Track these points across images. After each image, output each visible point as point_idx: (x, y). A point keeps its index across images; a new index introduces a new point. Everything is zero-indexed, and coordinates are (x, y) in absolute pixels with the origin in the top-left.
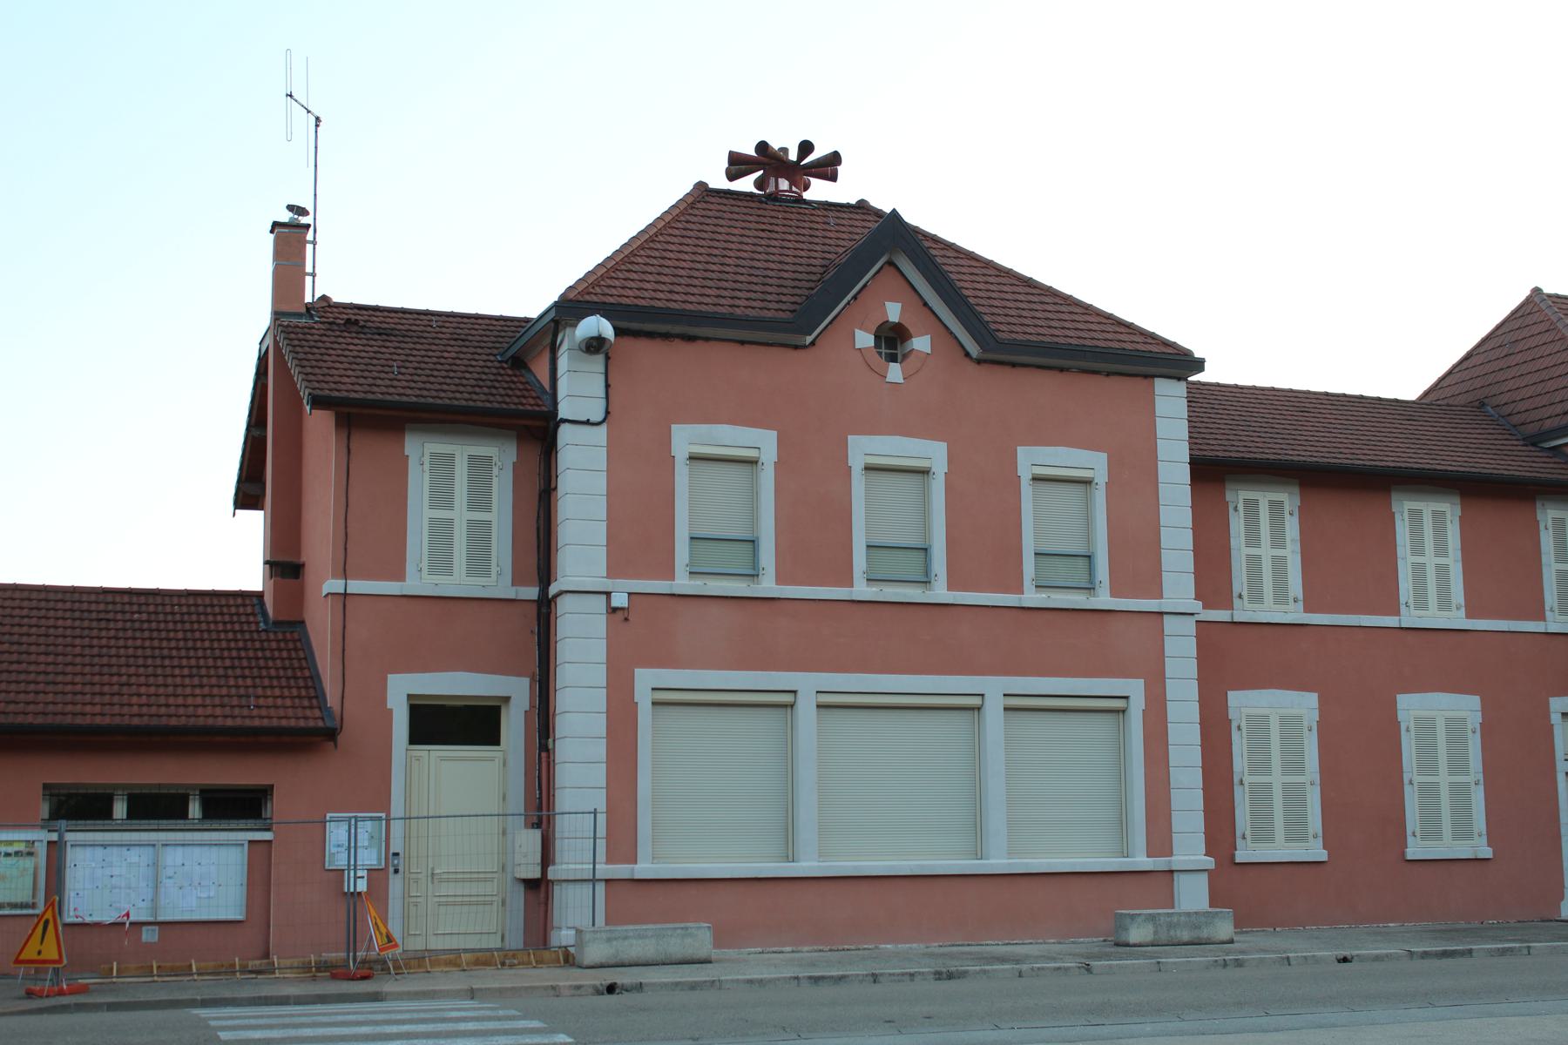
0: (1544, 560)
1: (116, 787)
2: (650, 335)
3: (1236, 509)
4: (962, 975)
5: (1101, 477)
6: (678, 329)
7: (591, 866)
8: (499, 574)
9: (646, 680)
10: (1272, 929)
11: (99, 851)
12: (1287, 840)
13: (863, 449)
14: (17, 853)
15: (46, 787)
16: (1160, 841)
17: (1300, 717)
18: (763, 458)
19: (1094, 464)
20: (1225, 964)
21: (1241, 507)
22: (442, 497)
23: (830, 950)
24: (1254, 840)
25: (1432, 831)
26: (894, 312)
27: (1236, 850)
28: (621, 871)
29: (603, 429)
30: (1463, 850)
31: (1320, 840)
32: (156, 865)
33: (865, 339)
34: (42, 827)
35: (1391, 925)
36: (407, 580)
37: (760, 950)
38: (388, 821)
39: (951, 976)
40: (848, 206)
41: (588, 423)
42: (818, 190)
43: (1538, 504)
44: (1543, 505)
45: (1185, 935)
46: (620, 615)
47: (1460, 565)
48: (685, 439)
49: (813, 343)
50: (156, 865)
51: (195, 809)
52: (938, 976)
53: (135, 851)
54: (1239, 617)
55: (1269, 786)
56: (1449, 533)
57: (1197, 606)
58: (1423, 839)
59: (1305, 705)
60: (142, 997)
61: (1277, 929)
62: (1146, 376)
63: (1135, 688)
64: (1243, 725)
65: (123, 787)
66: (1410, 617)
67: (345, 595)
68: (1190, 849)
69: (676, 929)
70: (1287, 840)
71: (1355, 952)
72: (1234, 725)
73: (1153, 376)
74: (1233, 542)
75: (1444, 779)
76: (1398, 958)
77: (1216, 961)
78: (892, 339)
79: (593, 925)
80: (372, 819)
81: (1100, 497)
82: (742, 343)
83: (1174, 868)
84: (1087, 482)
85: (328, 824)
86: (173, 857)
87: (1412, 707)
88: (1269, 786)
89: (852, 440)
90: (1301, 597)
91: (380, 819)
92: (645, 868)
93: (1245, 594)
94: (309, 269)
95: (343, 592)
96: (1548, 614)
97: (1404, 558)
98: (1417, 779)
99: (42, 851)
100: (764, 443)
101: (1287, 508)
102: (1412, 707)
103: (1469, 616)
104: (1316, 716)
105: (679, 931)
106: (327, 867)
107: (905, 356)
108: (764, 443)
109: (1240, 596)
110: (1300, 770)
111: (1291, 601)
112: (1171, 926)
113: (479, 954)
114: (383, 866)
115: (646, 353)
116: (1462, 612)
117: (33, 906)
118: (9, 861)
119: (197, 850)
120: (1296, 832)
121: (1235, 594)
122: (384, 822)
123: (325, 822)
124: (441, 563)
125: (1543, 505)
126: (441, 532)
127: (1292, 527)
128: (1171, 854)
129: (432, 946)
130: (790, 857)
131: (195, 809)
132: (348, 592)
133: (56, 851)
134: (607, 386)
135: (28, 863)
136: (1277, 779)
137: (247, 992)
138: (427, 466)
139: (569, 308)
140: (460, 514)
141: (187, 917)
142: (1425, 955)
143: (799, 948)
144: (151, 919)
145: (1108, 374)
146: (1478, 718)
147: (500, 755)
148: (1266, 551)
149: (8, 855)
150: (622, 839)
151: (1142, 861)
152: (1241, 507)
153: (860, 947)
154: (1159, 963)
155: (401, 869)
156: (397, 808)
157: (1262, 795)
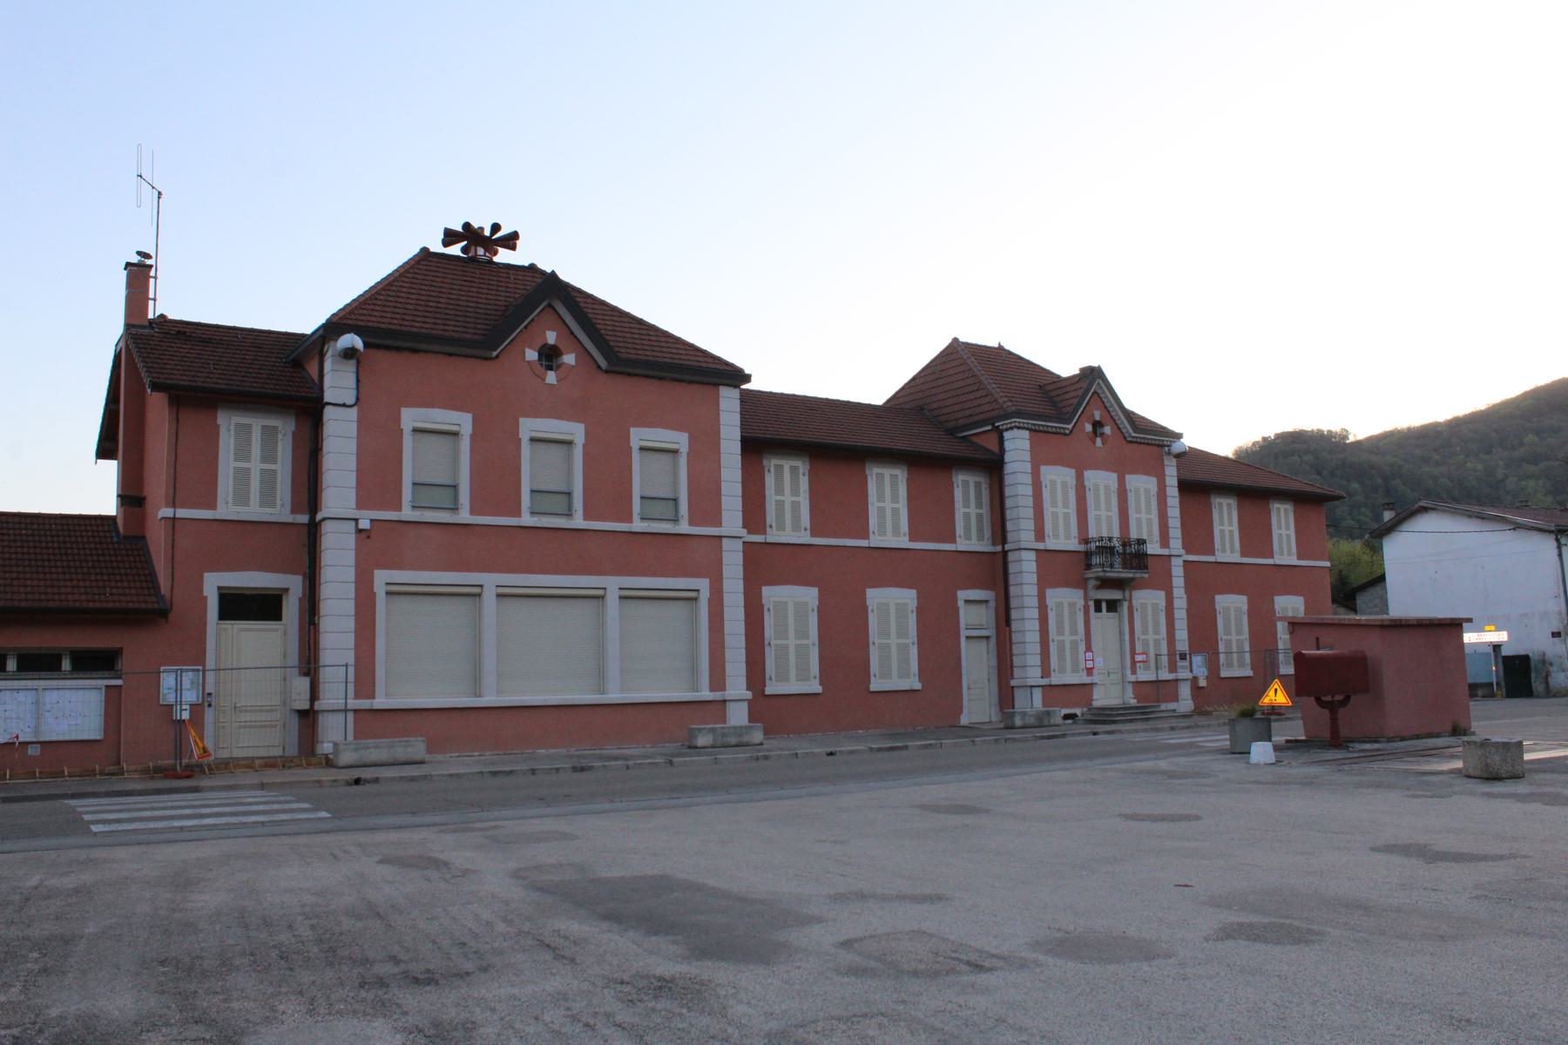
2: (388, 348)
3: (769, 471)
4: (590, 768)
6: (407, 344)
8: (282, 506)
9: (381, 578)
12: (797, 680)
13: (529, 427)
16: (718, 681)
17: (807, 603)
18: (462, 432)
19: (679, 440)
21: (772, 469)
22: (243, 453)
23: (505, 754)
25: (886, 674)
26: (551, 338)
28: (364, 704)
29: (355, 410)
30: (904, 685)
31: (818, 680)
33: (532, 355)
35: (860, 731)
36: (218, 508)
37: (457, 754)
38: (204, 671)
39: (582, 769)
41: (344, 405)
42: (503, 256)
43: (954, 472)
45: (733, 740)
46: (364, 535)
48: (411, 417)
49: (497, 356)
50: (37, 703)
51: (66, 665)
52: (575, 769)
53: (22, 694)
54: (770, 539)
58: (880, 678)
59: (810, 595)
60: (29, 793)
63: (703, 585)
66: (875, 541)
67: (174, 519)
68: (737, 686)
69: (400, 742)
70: (797, 680)
73: (717, 385)
74: (767, 492)
75: (894, 641)
78: (550, 356)
79: (346, 739)
80: (193, 670)
82: (450, 355)
83: (727, 698)
84: (675, 452)
85: (161, 674)
86: (51, 698)
87: (876, 597)
90: (808, 526)
91: (198, 670)
92: (380, 702)
93: (774, 524)
94: (151, 295)
95: (172, 516)
96: (958, 539)
97: (872, 504)
100: (463, 422)
101: (801, 471)
102: (876, 597)
105: (403, 743)
106: (161, 702)
107: (558, 367)
108: (463, 422)
109: (771, 526)
110: (805, 635)
111: (803, 529)
112: (724, 735)
114: (200, 702)
115: (384, 360)
116: (907, 538)
120: (803, 675)
124: (242, 497)
126: (242, 477)
127: (804, 484)
128: (724, 689)
129: (234, 755)
130: (477, 694)
131: (66, 665)
132: (177, 516)
138: (233, 433)
139: (333, 328)
140: (256, 465)
141: (61, 738)
142: (880, 750)
144: (34, 740)
145: (690, 382)
146: (915, 603)
148: (788, 498)
150: (364, 681)
151: (706, 694)
152: (772, 469)
154: (716, 758)
156: (210, 662)
157: (782, 651)
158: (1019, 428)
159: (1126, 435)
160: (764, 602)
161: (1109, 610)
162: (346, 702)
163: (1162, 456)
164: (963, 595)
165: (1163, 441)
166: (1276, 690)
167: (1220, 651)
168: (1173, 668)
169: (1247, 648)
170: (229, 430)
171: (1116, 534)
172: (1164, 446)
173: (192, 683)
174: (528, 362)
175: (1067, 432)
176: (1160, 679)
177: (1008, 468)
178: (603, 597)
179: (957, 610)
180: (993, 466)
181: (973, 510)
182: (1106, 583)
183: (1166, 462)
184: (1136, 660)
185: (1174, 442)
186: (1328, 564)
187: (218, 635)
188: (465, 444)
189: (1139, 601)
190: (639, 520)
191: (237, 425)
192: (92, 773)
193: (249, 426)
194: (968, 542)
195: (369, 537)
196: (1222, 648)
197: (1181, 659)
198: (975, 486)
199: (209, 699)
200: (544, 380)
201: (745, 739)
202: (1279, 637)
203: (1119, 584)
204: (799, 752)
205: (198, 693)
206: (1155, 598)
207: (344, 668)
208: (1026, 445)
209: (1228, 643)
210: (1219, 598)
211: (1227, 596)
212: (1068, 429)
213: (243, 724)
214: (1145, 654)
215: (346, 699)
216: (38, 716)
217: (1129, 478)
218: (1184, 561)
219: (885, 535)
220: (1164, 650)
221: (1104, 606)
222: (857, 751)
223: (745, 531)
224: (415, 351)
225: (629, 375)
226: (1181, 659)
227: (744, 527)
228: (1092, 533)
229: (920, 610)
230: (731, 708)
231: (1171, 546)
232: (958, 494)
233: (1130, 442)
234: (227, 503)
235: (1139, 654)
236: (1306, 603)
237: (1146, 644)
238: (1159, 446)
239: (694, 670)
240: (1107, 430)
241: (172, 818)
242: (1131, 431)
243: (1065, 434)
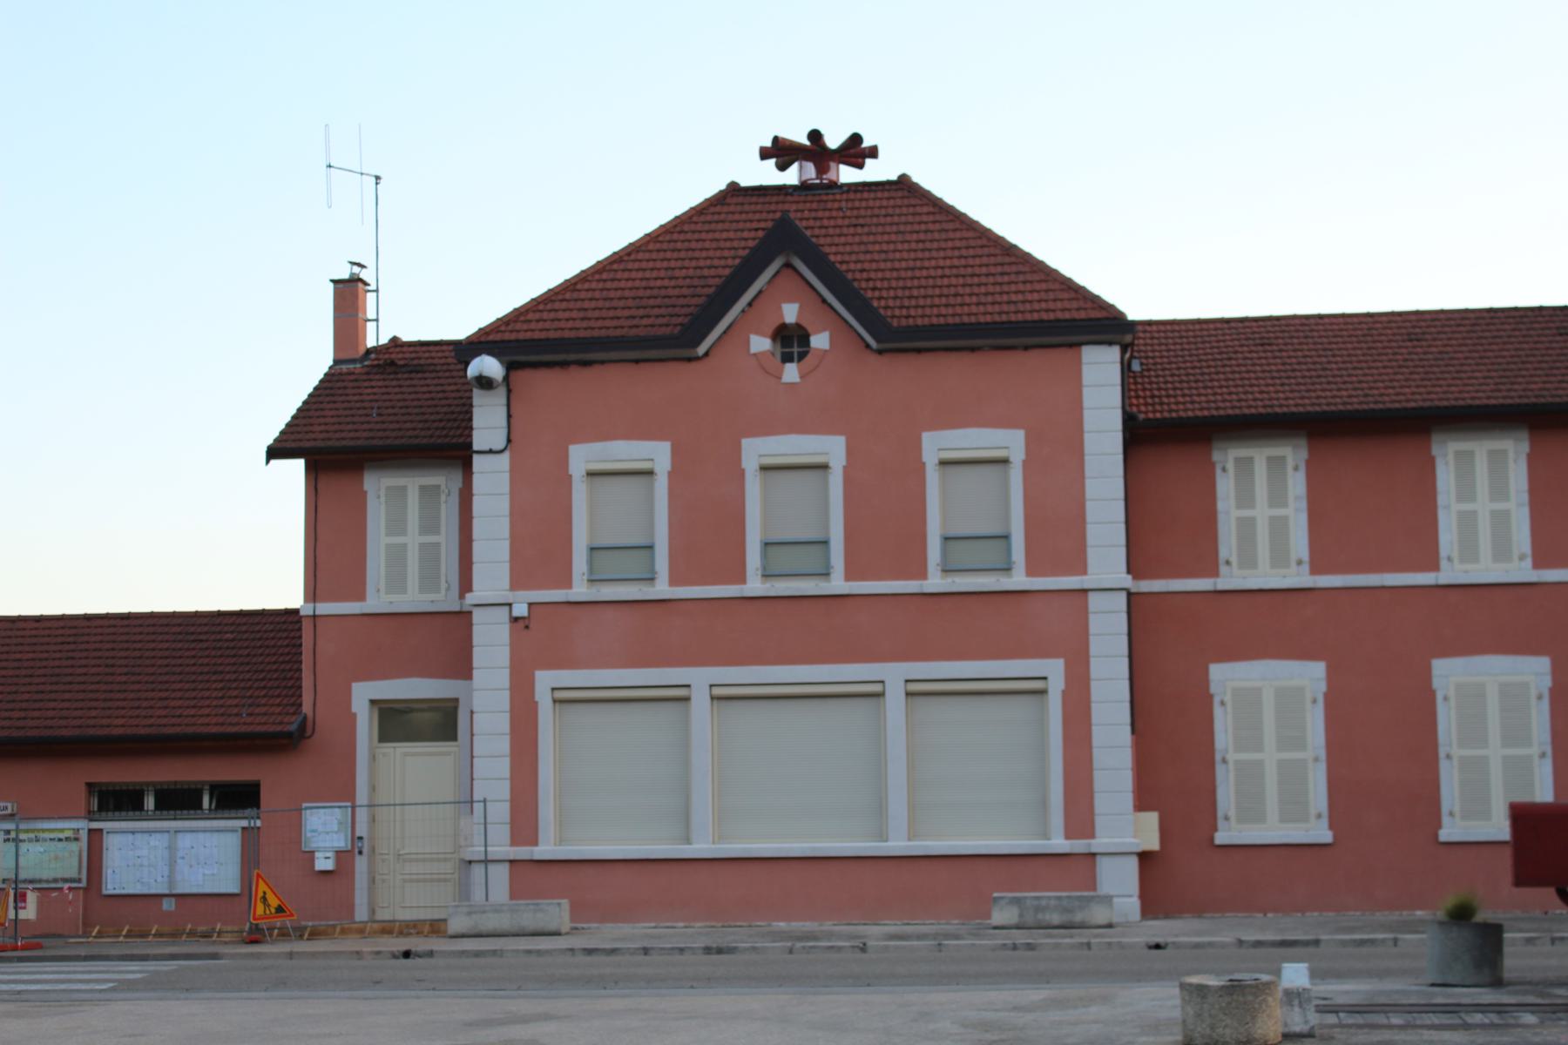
1: (203, 783)
3: (1224, 470)
4: (731, 951)
5: (1017, 454)
6: (572, 357)
7: (483, 849)
8: (448, 589)
9: (545, 680)
11: (130, 837)
12: (1282, 820)
13: (756, 450)
14: (67, 839)
15: (89, 785)
18: (657, 469)
19: (1011, 442)
20: (1015, 947)
21: (1230, 466)
22: (397, 525)
23: (723, 927)
25: (1252, 811)
26: (790, 313)
28: (523, 852)
29: (506, 457)
32: (172, 849)
33: (761, 344)
34: (85, 818)
35: (1419, 913)
37: (653, 925)
38: (353, 808)
39: (720, 951)
40: (889, 183)
41: (491, 452)
42: (847, 175)
45: (1056, 918)
46: (521, 624)
47: (1526, 511)
48: (582, 457)
49: (706, 354)
50: (172, 849)
51: (150, 802)
52: (708, 950)
54: (1223, 583)
55: (1260, 763)
57: (1127, 581)
59: (1310, 676)
60: (104, 951)
62: (1071, 345)
63: (1054, 670)
64: (1228, 698)
65: (153, 784)
66: (1448, 574)
67: (314, 616)
69: (528, 904)
70: (1282, 820)
71: (1170, 940)
72: (1216, 700)
73: (1080, 344)
74: (1220, 506)
75: (1271, 756)
76: (1223, 945)
77: (1005, 945)
78: (791, 341)
79: (487, 900)
80: (340, 807)
82: (637, 361)
83: (1094, 850)
84: (1004, 461)
85: (303, 812)
86: (185, 841)
87: (1448, 673)
88: (1260, 763)
89: (745, 442)
90: (1305, 555)
91: (346, 807)
92: (545, 849)
93: (1234, 560)
94: (371, 314)
95: (311, 613)
97: (1447, 507)
98: (1457, 752)
99: (84, 835)
100: (658, 455)
101: (1290, 463)
102: (1448, 673)
103: (1538, 564)
104: (1323, 687)
105: (532, 907)
106: (303, 849)
107: (802, 356)
108: (658, 455)
109: (1228, 563)
110: (1300, 744)
111: (1293, 564)
112: (1038, 909)
113: (384, 924)
114: (349, 848)
115: (542, 384)
116: (1528, 562)
117: (79, 881)
118: (60, 845)
119: (201, 836)
120: (1293, 809)
122: (350, 809)
123: (301, 810)
126: (397, 557)
127: (1297, 484)
128: (1092, 835)
129: (401, 917)
130: (882, 836)
131: (150, 802)
132: (317, 613)
133: (95, 836)
134: (509, 416)
135: (74, 846)
136: (1271, 756)
137: (83, 952)
138: (383, 499)
139: (481, 343)
140: (413, 539)
141: (194, 890)
142: (1258, 944)
143: (692, 924)
144: (167, 892)
145: (1026, 348)
146: (1547, 682)
147: (456, 749)
148: (1262, 512)
149: (60, 840)
150: (524, 824)
151: (1058, 843)
152: (1230, 466)
153: (754, 924)
154: (939, 945)
155: (365, 850)
156: (362, 796)
157: (1251, 775)
160: (1213, 689)
162: (486, 851)
170: (379, 497)
173: (340, 823)
174: (755, 355)
178: (880, 695)
187: (373, 758)
188: (661, 484)
190: (939, 573)
191: (388, 488)
192: (144, 935)
193: (404, 489)
195: (527, 627)
199: (360, 845)
200: (780, 378)
201: (1078, 917)
204: (1093, 941)
205: (346, 836)
207: (482, 804)
213: (407, 877)
215: (486, 846)
216: (172, 863)
219: (1476, 560)
222: (1372, 942)
223: (1130, 577)
224: (586, 364)
225: (919, 351)
230: (1103, 865)
234: (378, 590)
239: (880, 809)
241: (69, 981)
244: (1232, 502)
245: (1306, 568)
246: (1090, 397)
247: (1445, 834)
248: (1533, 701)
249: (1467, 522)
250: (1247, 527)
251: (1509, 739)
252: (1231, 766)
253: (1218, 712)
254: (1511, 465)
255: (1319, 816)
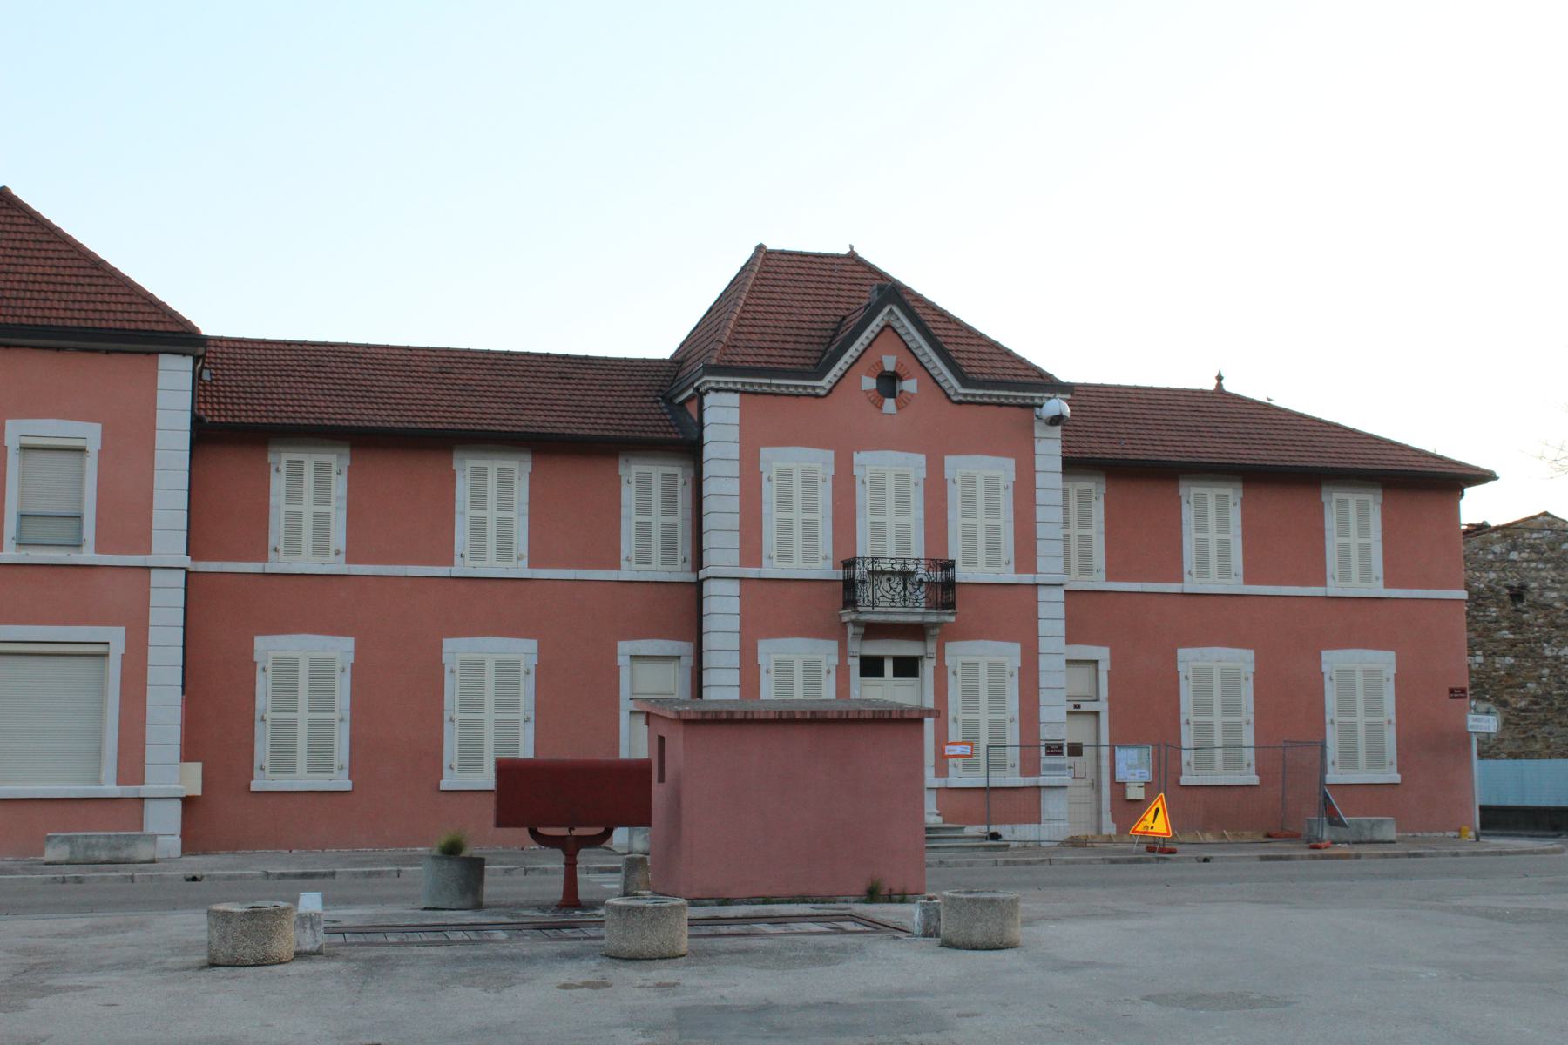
0: (624, 511)
3: (277, 470)
10: (288, 851)
12: (309, 772)
17: (333, 660)
19: (90, 434)
20: (64, 881)
21: (283, 467)
24: (272, 771)
25: (284, 763)
27: (253, 779)
35: (419, 849)
43: (622, 460)
44: (627, 461)
45: (104, 855)
54: (270, 568)
56: (516, 488)
57: (186, 562)
58: (461, 771)
59: (341, 649)
61: (294, 851)
62: (148, 353)
63: (115, 636)
64: (269, 666)
66: (461, 568)
70: (309, 772)
71: (205, 873)
72: (259, 667)
73: (157, 353)
74: (272, 500)
76: (253, 877)
77: (55, 878)
81: (91, 464)
84: (82, 450)
90: (343, 548)
93: (281, 547)
96: (624, 563)
97: (463, 513)
98: (458, 716)
101: (335, 468)
103: (531, 565)
104: (351, 658)
110: (329, 707)
120: (320, 761)
121: (271, 547)
125: (627, 461)
127: (339, 486)
142: (283, 876)
145: (108, 352)
151: (111, 789)
158: (717, 390)
159: (951, 392)
160: (256, 658)
161: (898, 672)
163: (1033, 421)
164: (625, 648)
165: (1032, 398)
166: (1157, 810)
167: (1185, 744)
168: (1030, 766)
169: (1248, 737)
171: (917, 549)
172: (1032, 406)
175: (822, 392)
176: (991, 785)
177: (708, 451)
179: (615, 672)
180: (689, 449)
181: (657, 519)
182: (874, 631)
183: (1037, 433)
184: (947, 753)
185: (1049, 398)
186: (1463, 595)
189: (961, 659)
194: (670, 568)
196: (1188, 738)
197: (1047, 754)
198: (663, 483)
201: (124, 854)
202: (1328, 718)
203: (916, 632)
204: (136, 874)
206: (1009, 654)
208: (734, 416)
209: (1204, 730)
210: (1184, 654)
211: (1206, 650)
212: (823, 388)
214: (972, 745)
217: (950, 461)
218: (1067, 591)
220: (1013, 735)
221: (889, 667)
222: (379, 874)
223: (189, 558)
226: (1047, 754)
227: (188, 554)
228: (864, 549)
229: (544, 672)
231: (1039, 571)
232: (629, 495)
233: (960, 403)
235: (955, 744)
236: (1258, 660)
237: (971, 727)
238: (1022, 406)
240: (909, 386)
242: (956, 384)
243: (817, 396)
244: (283, 498)
245: (342, 557)
246: (163, 399)
247: (445, 784)
248: (522, 674)
249: (478, 526)
250: (294, 520)
251: (499, 708)
252: (268, 722)
253: (260, 677)
254: (516, 481)
255: (341, 768)
